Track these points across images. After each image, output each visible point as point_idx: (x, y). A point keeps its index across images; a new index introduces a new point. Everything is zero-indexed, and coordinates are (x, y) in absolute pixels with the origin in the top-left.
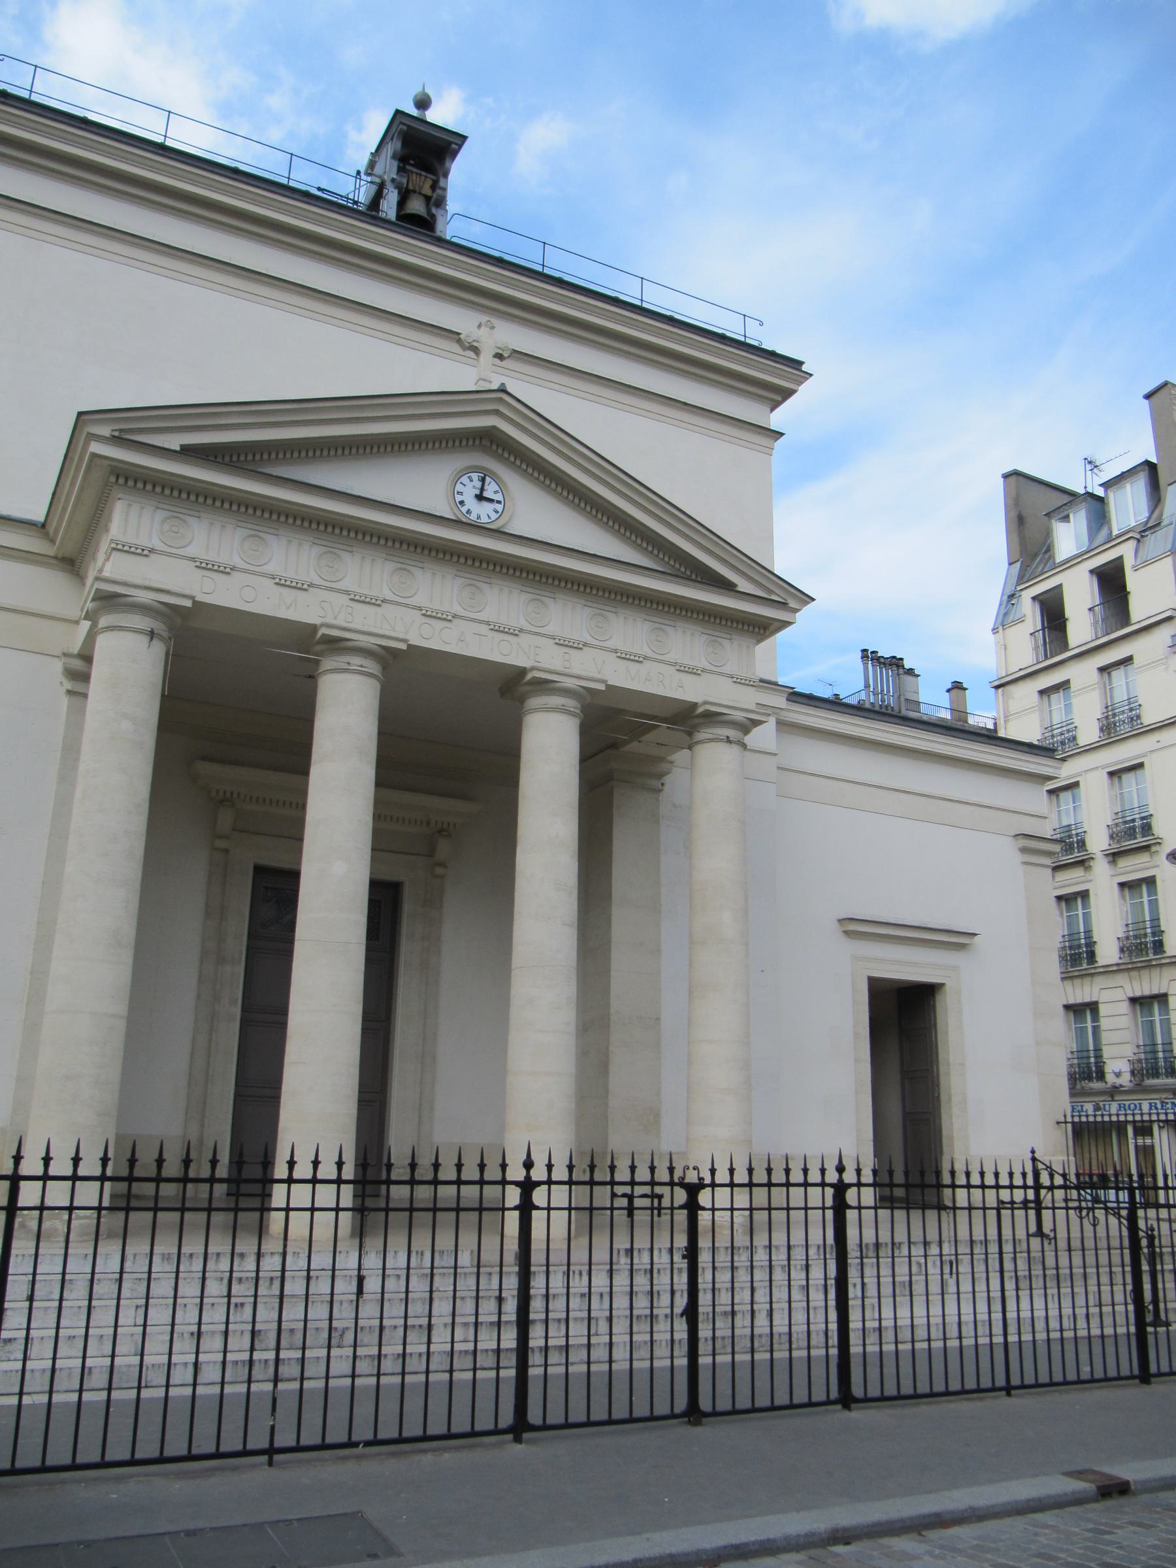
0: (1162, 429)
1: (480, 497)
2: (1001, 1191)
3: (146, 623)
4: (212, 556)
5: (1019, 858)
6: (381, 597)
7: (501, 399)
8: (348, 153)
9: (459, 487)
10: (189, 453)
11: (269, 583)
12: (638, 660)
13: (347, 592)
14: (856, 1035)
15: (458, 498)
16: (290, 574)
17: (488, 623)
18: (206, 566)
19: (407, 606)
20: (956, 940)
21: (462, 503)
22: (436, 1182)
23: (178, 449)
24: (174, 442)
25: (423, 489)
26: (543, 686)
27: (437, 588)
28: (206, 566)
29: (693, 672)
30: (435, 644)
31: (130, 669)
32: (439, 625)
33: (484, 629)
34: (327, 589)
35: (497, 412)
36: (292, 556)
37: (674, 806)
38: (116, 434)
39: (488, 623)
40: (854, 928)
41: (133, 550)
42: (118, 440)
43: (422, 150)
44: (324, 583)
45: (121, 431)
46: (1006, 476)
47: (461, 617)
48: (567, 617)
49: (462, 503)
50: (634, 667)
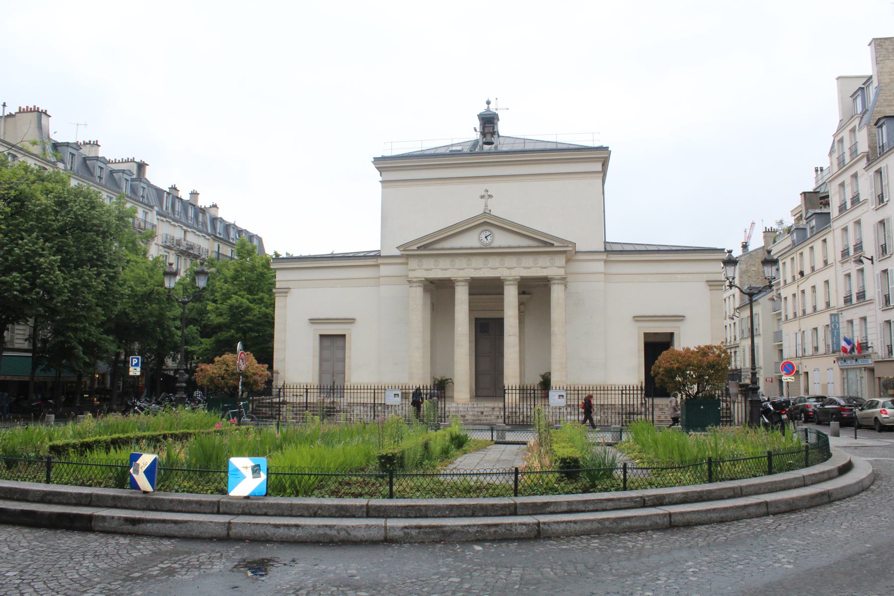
0: (879, 60)
5: (708, 288)
8: (468, 132)
12: (529, 268)
14: (639, 350)
18: (426, 270)
20: (680, 318)
24: (415, 247)
25: (471, 240)
27: (477, 262)
28: (426, 270)
29: (545, 268)
31: (418, 292)
36: (444, 263)
40: (637, 319)
42: (404, 250)
43: (488, 122)
46: (837, 79)
48: (510, 261)
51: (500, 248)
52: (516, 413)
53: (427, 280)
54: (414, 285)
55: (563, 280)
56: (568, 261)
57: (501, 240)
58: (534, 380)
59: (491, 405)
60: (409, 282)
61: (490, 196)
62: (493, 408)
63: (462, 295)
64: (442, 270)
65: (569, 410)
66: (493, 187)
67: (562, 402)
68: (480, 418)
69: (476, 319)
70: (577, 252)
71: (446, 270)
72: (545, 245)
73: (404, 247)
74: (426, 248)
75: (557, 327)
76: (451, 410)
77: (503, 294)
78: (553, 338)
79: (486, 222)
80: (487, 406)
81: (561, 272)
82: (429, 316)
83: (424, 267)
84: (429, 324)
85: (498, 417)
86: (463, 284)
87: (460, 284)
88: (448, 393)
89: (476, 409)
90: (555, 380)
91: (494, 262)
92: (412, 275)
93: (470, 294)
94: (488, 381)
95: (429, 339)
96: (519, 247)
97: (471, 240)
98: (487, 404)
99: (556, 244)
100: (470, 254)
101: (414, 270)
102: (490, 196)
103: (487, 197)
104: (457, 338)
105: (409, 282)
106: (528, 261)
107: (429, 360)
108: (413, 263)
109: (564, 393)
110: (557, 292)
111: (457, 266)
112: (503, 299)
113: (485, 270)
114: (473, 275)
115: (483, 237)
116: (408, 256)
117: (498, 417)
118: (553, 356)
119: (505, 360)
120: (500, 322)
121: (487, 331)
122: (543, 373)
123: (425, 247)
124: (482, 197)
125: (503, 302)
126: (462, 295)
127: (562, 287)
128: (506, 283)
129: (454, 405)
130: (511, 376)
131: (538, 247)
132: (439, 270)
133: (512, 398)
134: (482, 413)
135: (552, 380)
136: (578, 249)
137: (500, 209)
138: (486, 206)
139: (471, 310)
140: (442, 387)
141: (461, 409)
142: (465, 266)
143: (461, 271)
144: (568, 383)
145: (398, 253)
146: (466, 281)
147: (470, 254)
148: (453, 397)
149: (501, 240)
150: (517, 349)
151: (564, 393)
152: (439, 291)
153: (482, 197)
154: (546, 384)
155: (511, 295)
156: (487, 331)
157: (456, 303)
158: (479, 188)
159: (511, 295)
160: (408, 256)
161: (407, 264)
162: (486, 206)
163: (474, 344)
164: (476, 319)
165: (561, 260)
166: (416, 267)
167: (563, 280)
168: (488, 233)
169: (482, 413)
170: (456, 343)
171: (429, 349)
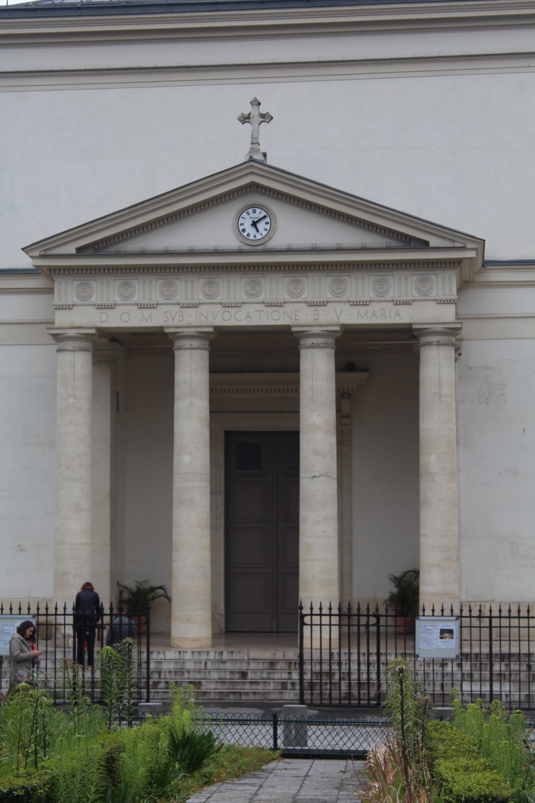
1: (254, 224)
2: (521, 620)
3: (77, 344)
4: (105, 301)
6: (197, 302)
7: (252, 166)
9: (241, 221)
10: (81, 251)
11: (135, 308)
12: (365, 304)
13: (178, 304)
15: (241, 228)
16: (147, 301)
17: (263, 303)
19: (213, 303)
21: (244, 230)
22: (47, 615)
23: (74, 252)
24: (71, 249)
25: (216, 232)
26: (304, 335)
27: (233, 288)
28: (101, 307)
29: (406, 303)
30: (232, 322)
32: (233, 310)
33: (261, 307)
34: (167, 304)
35: (252, 173)
37: (470, 368)
38: (42, 253)
39: (263, 303)
41: (64, 307)
42: (42, 256)
44: (166, 302)
45: (45, 250)
47: (246, 303)
48: (316, 287)
49: (244, 230)
50: (363, 309)
51: (289, 251)
52: (330, 674)
53: (102, 332)
54: (70, 345)
55: (452, 336)
56: (464, 285)
57: (293, 231)
58: (374, 589)
59: (267, 654)
60: (58, 338)
61: (266, 118)
62: (272, 663)
63: (191, 373)
64: (142, 307)
65: (467, 667)
66: (275, 94)
67: (449, 648)
68: (239, 688)
69: (228, 434)
70: (487, 264)
71: (151, 307)
72: (406, 245)
73: (42, 248)
74: (101, 250)
75: (435, 456)
76: (165, 666)
77: (295, 369)
78: (424, 484)
79: (255, 186)
80: (254, 656)
81: (447, 314)
82: (105, 427)
83: (93, 300)
84: (107, 446)
85: (284, 685)
86: (195, 343)
87: (187, 343)
88: (156, 625)
89: (229, 666)
90: (433, 588)
91: (275, 288)
92: (62, 319)
93: (213, 370)
94: (258, 589)
95: (107, 486)
96: (339, 250)
97: (216, 232)
98: (255, 653)
99: (434, 242)
100: (212, 267)
101: (69, 307)
102: (266, 118)
103: (256, 119)
104: (178, 483)
105: (58, 338)
106: (360, 286)
107: (107, 539)
108: (67, 291)
109: (454, 626)
110: (436, 367)
111: (179, 298)
112: (297, 382)
113: (252, 307)
114: (219, 322)
115: (246, 222)
116: (52, 272)
117: (284, 685)
118: (424, 531)
119: (304, 540)
120: (289, 443)
121: (257, 467)
122: (398, 573)
123: (95, 249)
124: (245, 119)
125: (297, 391)
126: (191, 373)
127: (450, 352)
128: (302, 342)
129: (171, 655)
130: (318, 578)
131: (388, 249)
132: (133, 308)
133: (320, 637)
134: (244, 675)
135: (423, 589)
136: (490, 254)
137: (289, 152)
138: (255, 142)
139: (217, 409)
140: (141, 609)
141: (189, 666)
142: (202, 298)
143: (190, 310)
144: (464, 598)
145: (26, 262)
146: (202, 336)
147: (212, 267)
148: (168, 634)
149: (293, 231)
150: (332, 510)
151: (454, 626)
152: (132, 365)
153: (245, 119)
154: (406, 600)
155: (317, 373)
156: (257, 467)
157: (177, 392)
158: (237, 95)
159: (317, 373)
160: (52, 272)
161: (50, 291)
162: (255, 142)
163: (221, 498)
164: (228, 434)
165: (445, 285)
166: (76, 300)
167: (452, 336)
168: (259, 213)
169: (244, 675)
170: (176, 494)
171: (106, 510)
